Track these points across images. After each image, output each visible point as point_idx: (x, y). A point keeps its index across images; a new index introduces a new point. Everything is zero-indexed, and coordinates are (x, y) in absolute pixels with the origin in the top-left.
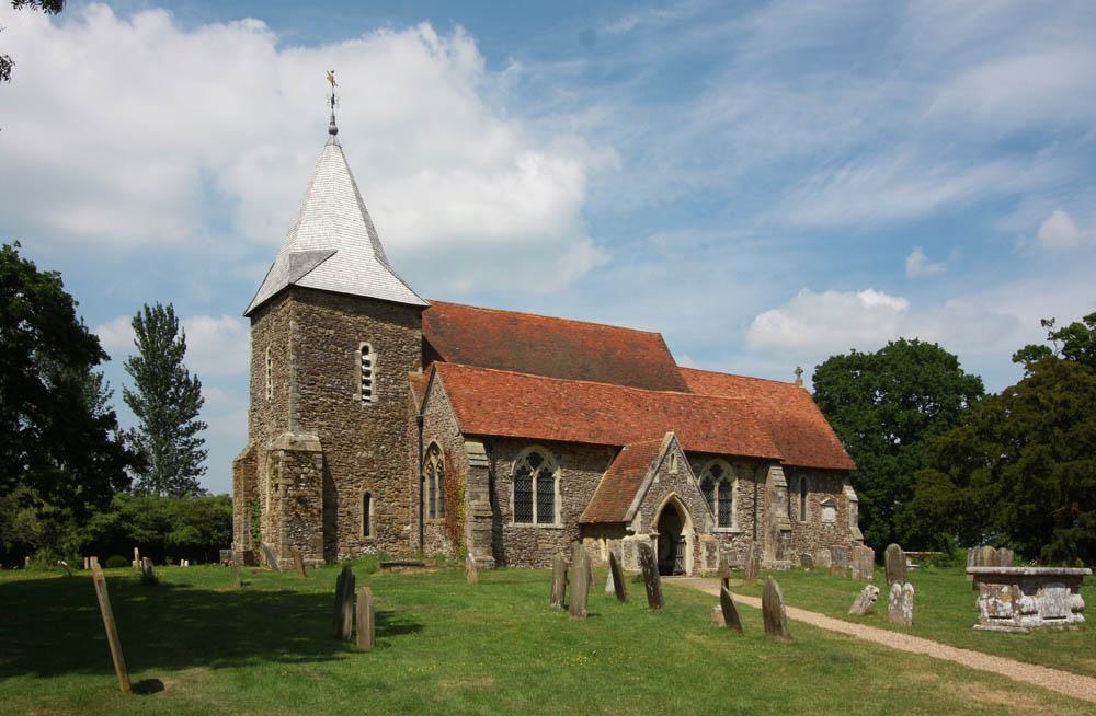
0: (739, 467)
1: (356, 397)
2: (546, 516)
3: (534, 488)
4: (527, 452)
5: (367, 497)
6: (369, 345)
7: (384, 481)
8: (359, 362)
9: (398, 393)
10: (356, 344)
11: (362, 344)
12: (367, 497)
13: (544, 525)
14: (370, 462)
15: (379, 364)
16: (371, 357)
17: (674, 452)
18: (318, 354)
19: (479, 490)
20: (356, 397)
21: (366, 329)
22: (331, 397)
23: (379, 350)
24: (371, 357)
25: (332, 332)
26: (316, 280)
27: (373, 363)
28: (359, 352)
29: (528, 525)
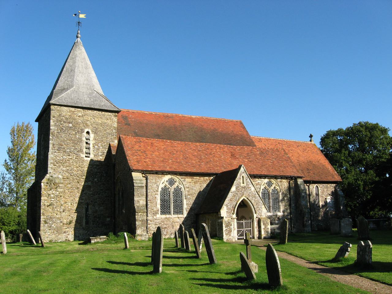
8: (84, 139)
10: (82, 131)
11: (86, 130)
13: (176, 216)
15: (95, 139)
16: (92, 136)
17: (243, 175)
18: (63, 135)
19: (139, 198)
21: (88, 122)
22: (69, 155)
23: (95, 133)
25: (71, 125)
29: (168, 216)
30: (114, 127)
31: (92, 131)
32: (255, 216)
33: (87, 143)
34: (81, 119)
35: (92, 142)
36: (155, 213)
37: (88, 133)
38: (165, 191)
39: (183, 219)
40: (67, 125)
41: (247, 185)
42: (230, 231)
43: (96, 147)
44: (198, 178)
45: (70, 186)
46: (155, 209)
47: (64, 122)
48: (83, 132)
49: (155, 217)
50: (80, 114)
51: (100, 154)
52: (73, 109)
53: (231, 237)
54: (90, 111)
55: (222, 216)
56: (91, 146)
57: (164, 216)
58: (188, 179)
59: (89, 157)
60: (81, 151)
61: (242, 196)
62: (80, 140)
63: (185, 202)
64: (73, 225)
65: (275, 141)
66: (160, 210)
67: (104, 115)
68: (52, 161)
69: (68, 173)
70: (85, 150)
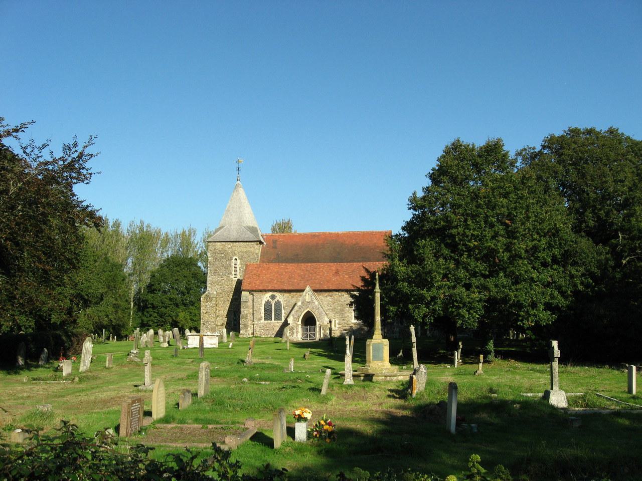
3: (273, 308)
10: (231, 259)
11: (234, 258)
15: (241, 264)
16: (239, 261)
20: (231, 276)
22: (222, 277)
25: (223, 255)
26: (219, 236)
29: (269, 321)
31: (239, 258)
32: (318, 323)
33: (235, 267)
34: (231, 249)
35: (238, 266)
36: (260, 319)
38: (268, 304)
39: (281, 324)
40: (220, 255)
41: (311, 300)
42: (293, 333)
43: (242, 269)
44: (295, 293)
45: (222, 299)
46: (259, 317)
47: (218, 253)
50: (229, 246)
52: (224, 243)
53: (293, 338)
54: (237, 243)
55: (289, 323)
56: (238, 269)
57: (266, 322)
58: (287, 295)
60: (231, 273)
61: (306, 309)
62: (230, 266)
63: (283, 311)
64: (224, 326)
66: (263, 317)
67: (248, 245)
68: (210, 282)
69: (221, 290)
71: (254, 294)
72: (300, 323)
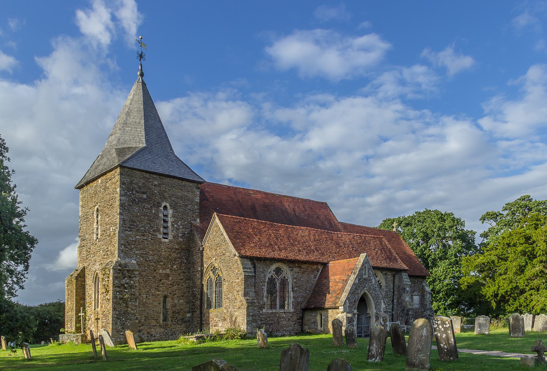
0: (386, 274)
1: (160, 236)
2: (282, 306)
4: (274, 267)
5: (165, 297)
6: (168, 205)
7: (175, 287)
8: (161, 215)
9: (184, 233)
10: (159, 205)
11: (164, 204)
12: (165, 297)
14: (168, 275)
15: (173, 216)
22: (144, 235)
23: (173, 207)
24: (170, 212)
27: (170, 216)
28: (162, 209)
29: (274, 311)
30: (196, 202)
31: (170, 206)
33: (164, 221)
35: (170, 220)
37: (165, 207)
38: (272, 281)
46: (261, 303)
48: (160, 206)
49: (261, 312)
50: (156, 183)
51: (180, 235)
52: (148, 175)
54: (168, 180)
56: (169, 224)
59: (167, 238)
60: (158, 230)
62: (156, 216)
65: (360, 228)
67: (185, 186)
69: (143, 257)
70: (162, 229)
71: (258, 265)
72: (355, 311)
